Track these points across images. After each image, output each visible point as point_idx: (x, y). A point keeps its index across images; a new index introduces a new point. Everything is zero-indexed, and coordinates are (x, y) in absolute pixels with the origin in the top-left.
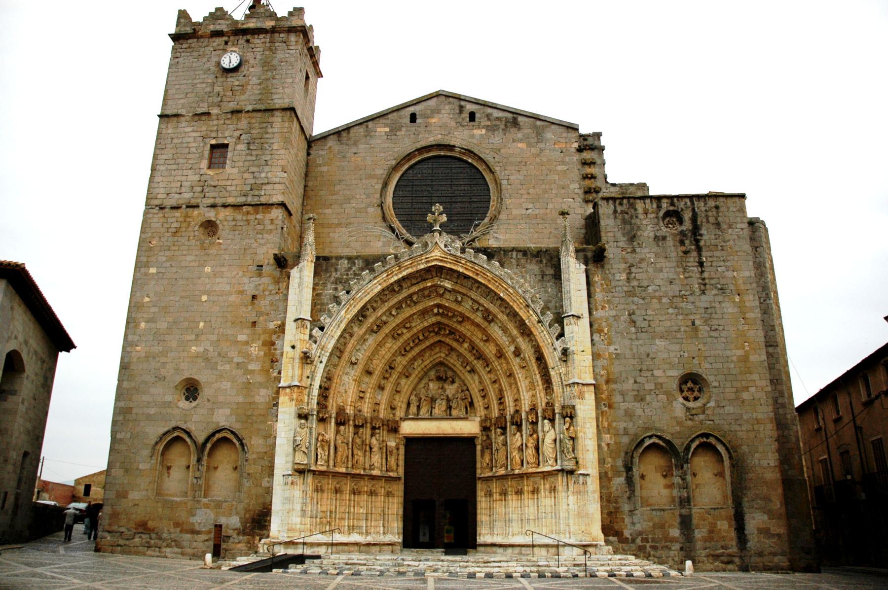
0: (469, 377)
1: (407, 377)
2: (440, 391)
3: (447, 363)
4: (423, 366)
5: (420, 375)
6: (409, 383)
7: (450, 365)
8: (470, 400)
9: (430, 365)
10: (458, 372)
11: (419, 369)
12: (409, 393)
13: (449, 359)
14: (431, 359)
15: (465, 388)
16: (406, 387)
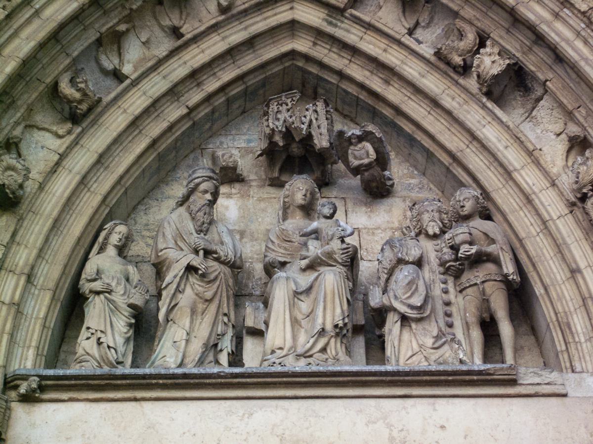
0: (491, 134)
1: (75, 118)
2: (296, 223)
3: (336, 60)
4: (178, 69)
5: (155, 129)
6: (82, 160)
7: (357, 72)
8: (509, 268)
9: (227, 75)
10: (416, 109)
11: (157, 85)
12: (77, 225)
13: (352, 35)
14: (236, 35)
15: (467, 198)
16: (62, 185)
